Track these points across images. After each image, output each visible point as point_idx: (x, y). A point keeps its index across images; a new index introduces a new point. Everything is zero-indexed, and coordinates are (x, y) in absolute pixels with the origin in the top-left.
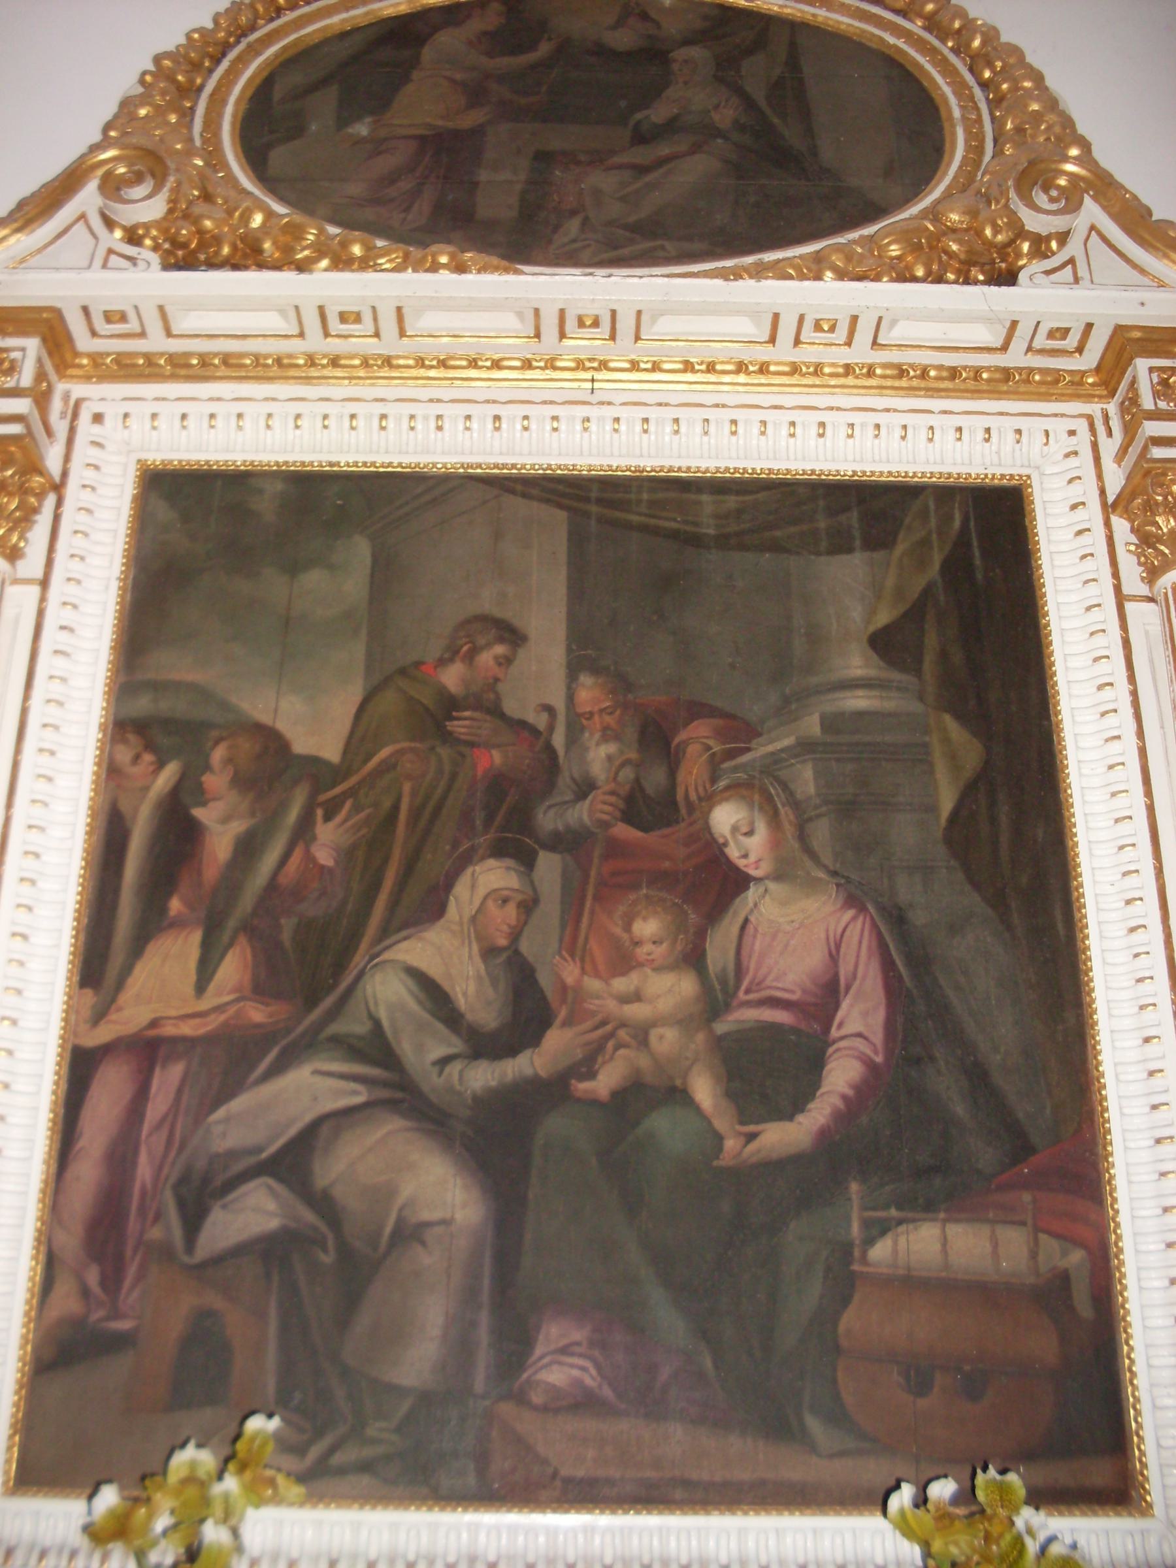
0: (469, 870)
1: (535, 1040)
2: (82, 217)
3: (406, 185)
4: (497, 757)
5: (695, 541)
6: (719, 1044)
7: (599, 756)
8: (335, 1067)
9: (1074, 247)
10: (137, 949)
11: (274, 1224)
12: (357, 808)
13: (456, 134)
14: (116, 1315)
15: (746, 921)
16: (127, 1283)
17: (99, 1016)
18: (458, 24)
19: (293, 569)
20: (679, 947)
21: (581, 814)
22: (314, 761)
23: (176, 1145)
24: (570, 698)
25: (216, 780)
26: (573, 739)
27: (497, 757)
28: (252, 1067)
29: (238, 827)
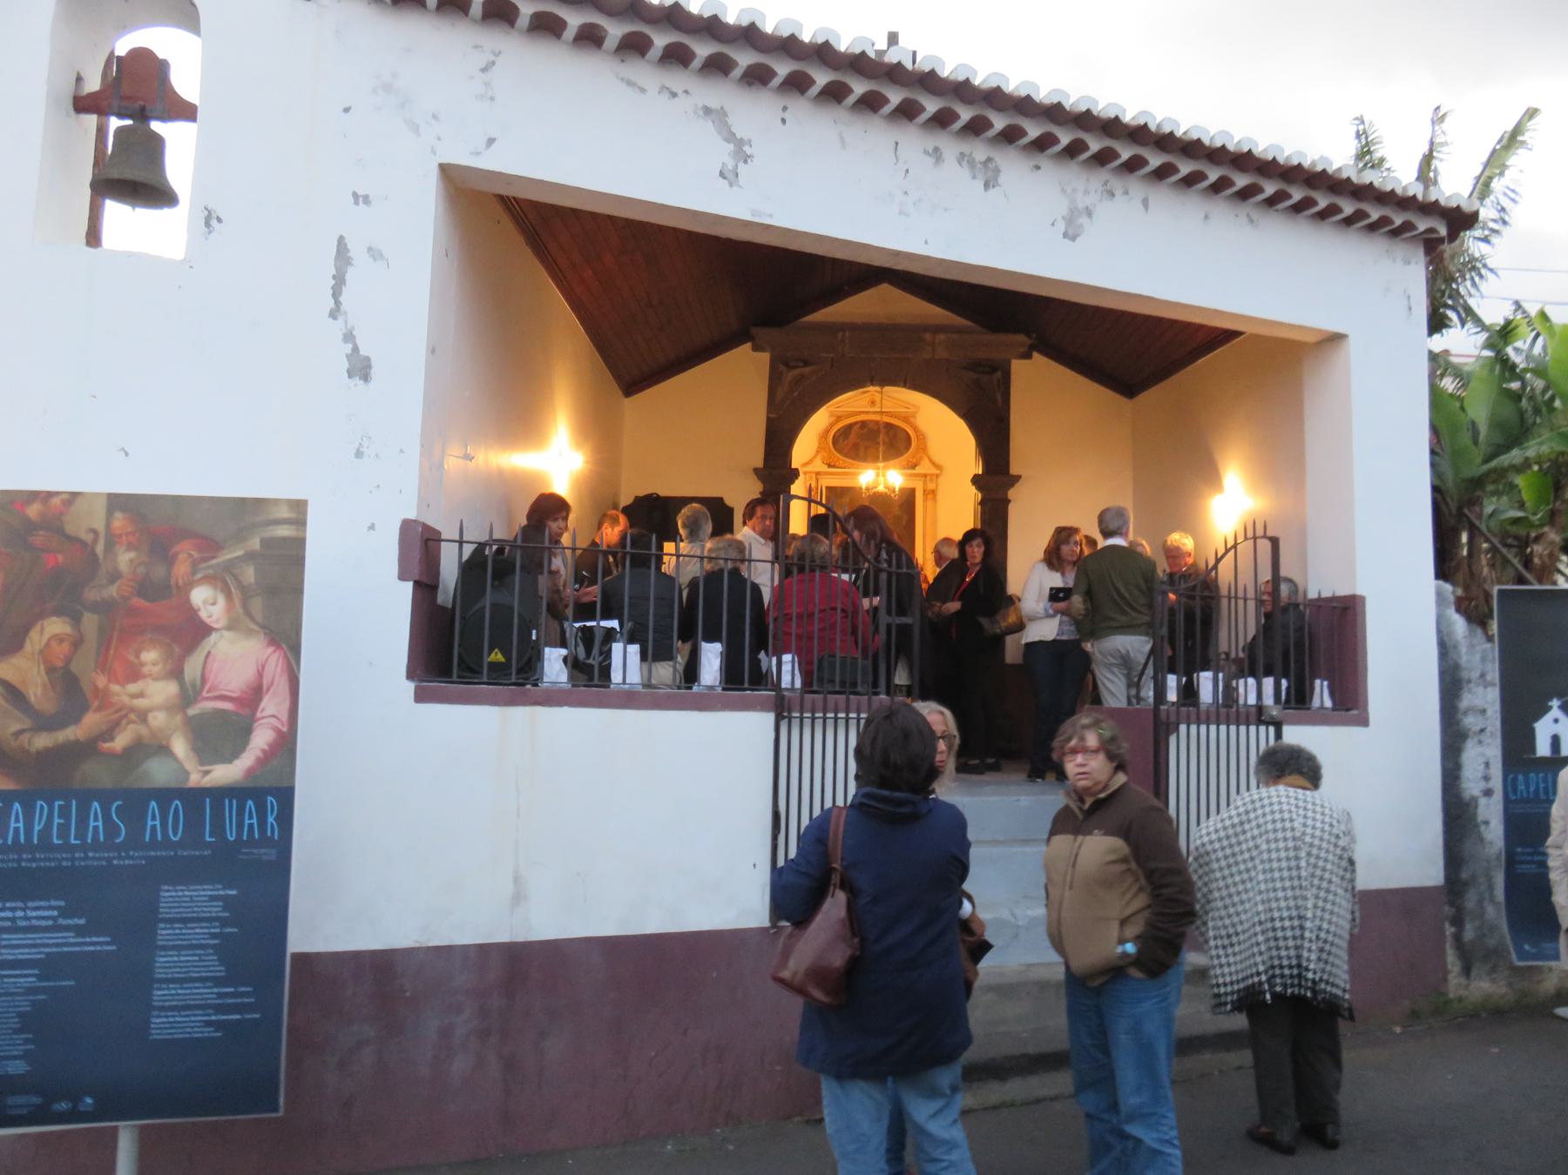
0: (39, 626)
1: (77, 720)
6: (189, 721)
7: (125, 559)
20: (169, 667)
21: (113, 591)
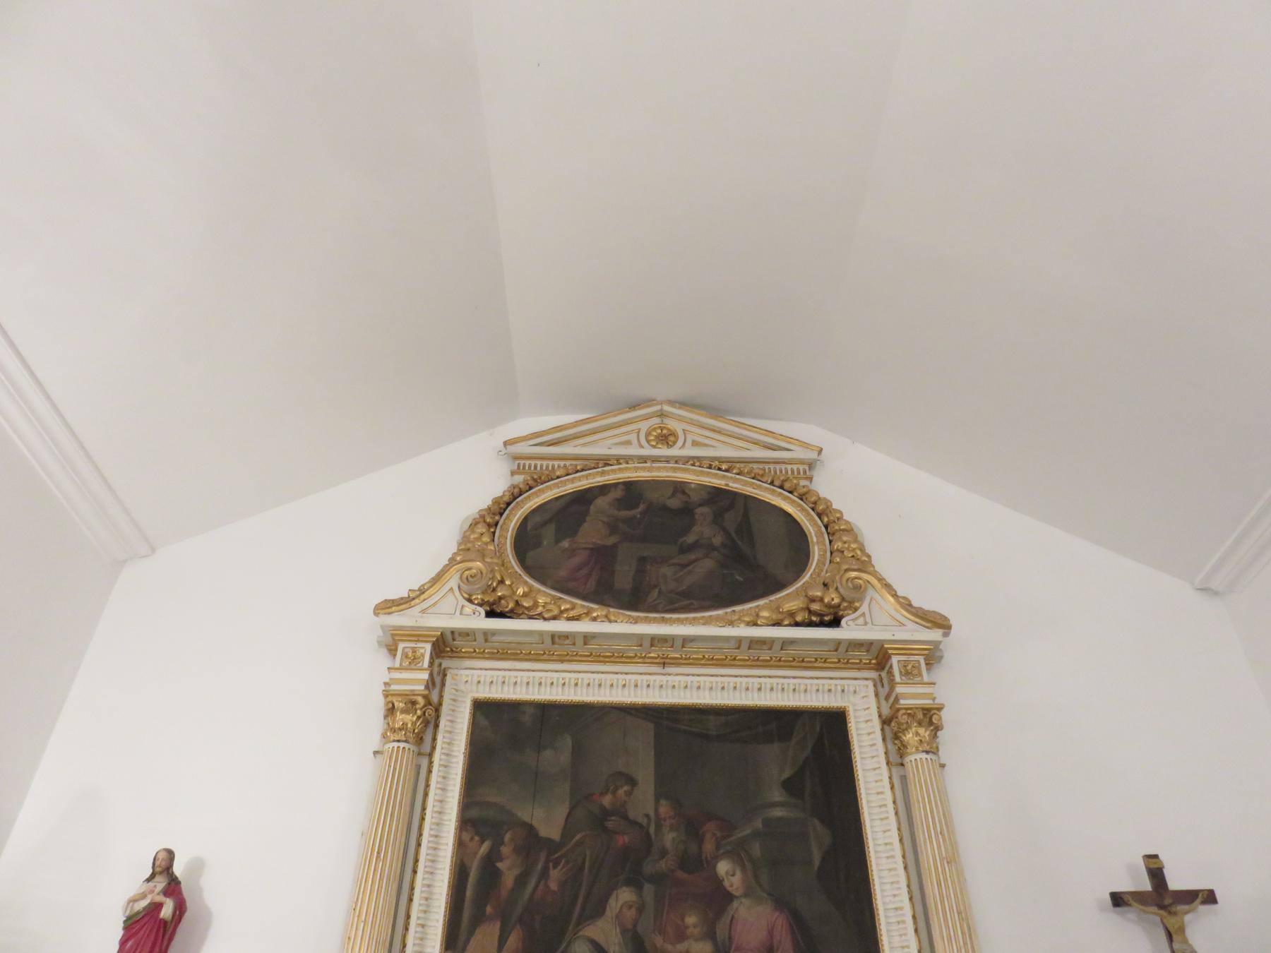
2: (451, 589)
3: (584, 571)
4: (626, 839)
5: (705, 737)
7: (669, 838)
9: (864, 608)
10: (471, 933)
12: (567, 862)
13: (605, 547)
15: (733, 917)
18: (604, 495)
19: (539, 749)
21: (663, 865)
22: (549, 840)
24: (656, 810)
25: (505, 850)
26: (659, 826)
27: (626, 839)
29: (516, 872)
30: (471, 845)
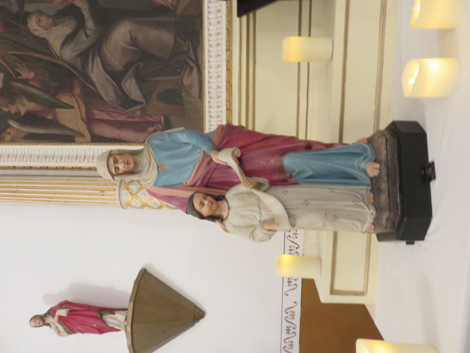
0: (32, 32)
1: (79, 9)
8: (90, 67)
11: (134, 81)
12: (17, 67)
14: (160, 122)
16: (152, 120)
17: (82, 135)
22: (4, 81)
23: (115, 110)
25: (13, 110)
28: (92, 90)
29: (25, 101)
30: (12, 134)
